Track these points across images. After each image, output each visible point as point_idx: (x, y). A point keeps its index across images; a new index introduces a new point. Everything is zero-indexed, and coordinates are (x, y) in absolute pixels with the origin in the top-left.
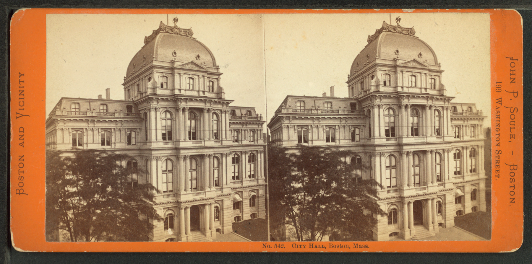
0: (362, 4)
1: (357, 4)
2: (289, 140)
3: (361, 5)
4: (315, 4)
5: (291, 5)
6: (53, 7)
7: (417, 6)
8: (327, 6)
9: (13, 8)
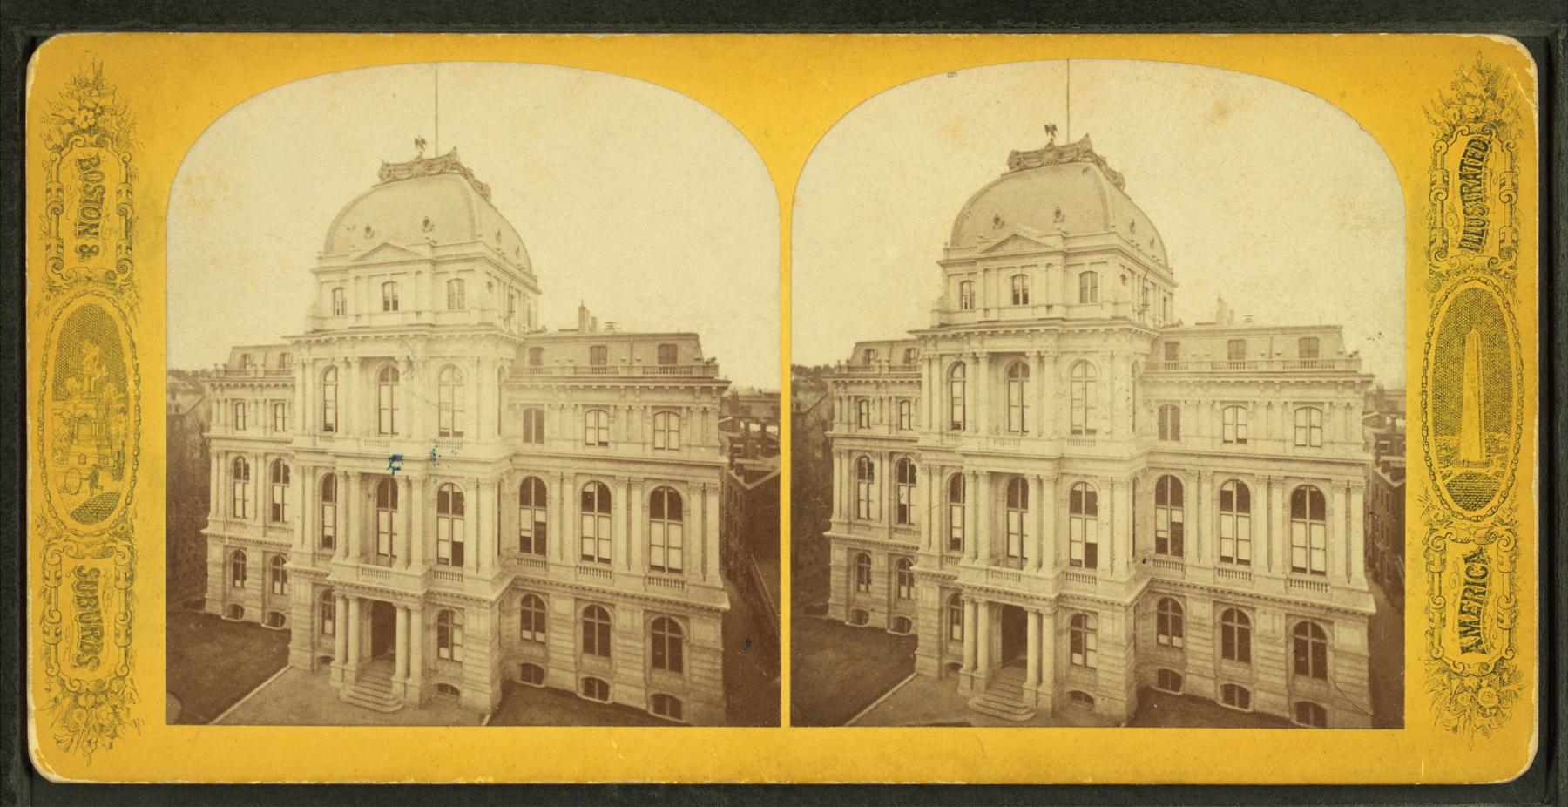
0: (1040, 21)
1: (1024, 20)
2: (1199, 435)
3: (1035, 24)
4: (905, 19)
5: (834, 23)
6: (150, 30)
7: (1195, 24)
8: (936, 27)
9: (35, 34)
